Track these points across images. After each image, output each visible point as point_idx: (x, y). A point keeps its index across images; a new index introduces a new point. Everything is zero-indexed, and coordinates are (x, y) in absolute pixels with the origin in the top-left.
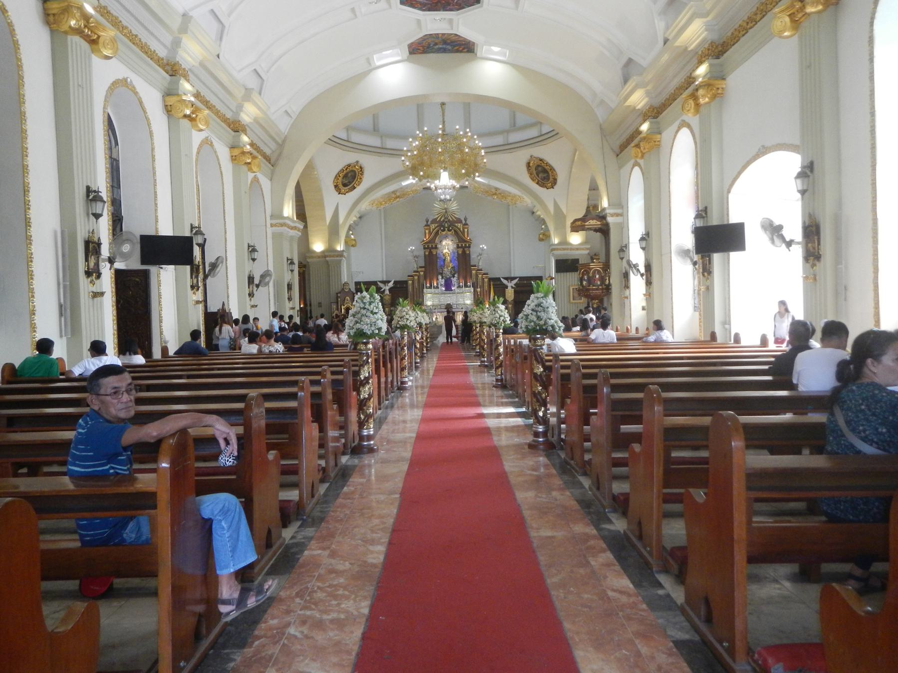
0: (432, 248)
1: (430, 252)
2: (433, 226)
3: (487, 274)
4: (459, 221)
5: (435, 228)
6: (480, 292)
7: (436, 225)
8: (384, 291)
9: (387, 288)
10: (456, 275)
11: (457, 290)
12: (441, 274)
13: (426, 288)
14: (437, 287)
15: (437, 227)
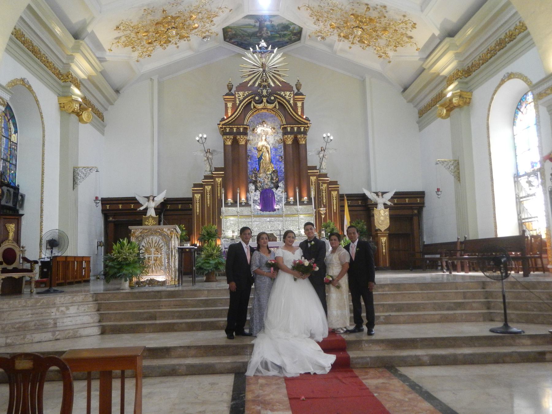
0: (239, 133)
1: (235, 142)
2: (241, 94)
3: (335, 183)
4: (287, 87)
5: (244, 99)
6: (325, 214)
7: (247, 93)
8: (146, 209)
9: (152, 205)
10: (281, 184)
11: (287, 210)
12: (255, 183)
13: (226, 205)
14: (247, 205)
15: (247, 96)
